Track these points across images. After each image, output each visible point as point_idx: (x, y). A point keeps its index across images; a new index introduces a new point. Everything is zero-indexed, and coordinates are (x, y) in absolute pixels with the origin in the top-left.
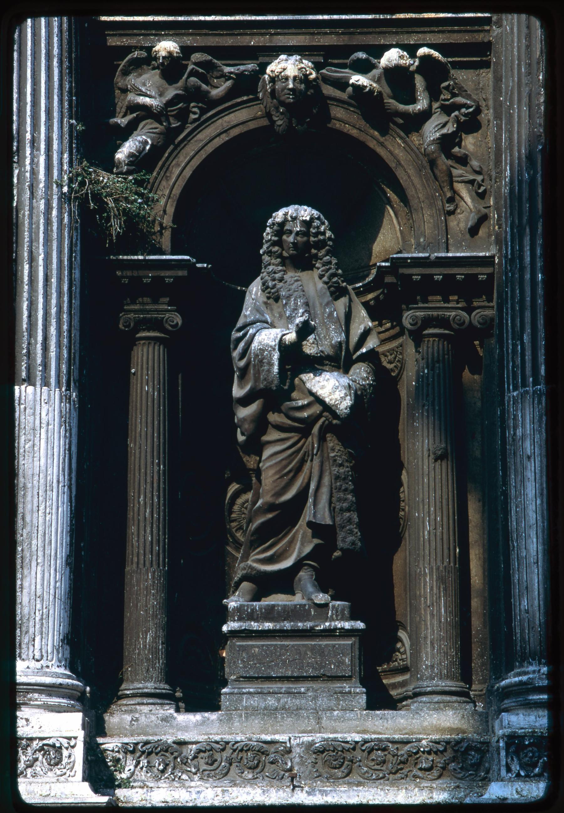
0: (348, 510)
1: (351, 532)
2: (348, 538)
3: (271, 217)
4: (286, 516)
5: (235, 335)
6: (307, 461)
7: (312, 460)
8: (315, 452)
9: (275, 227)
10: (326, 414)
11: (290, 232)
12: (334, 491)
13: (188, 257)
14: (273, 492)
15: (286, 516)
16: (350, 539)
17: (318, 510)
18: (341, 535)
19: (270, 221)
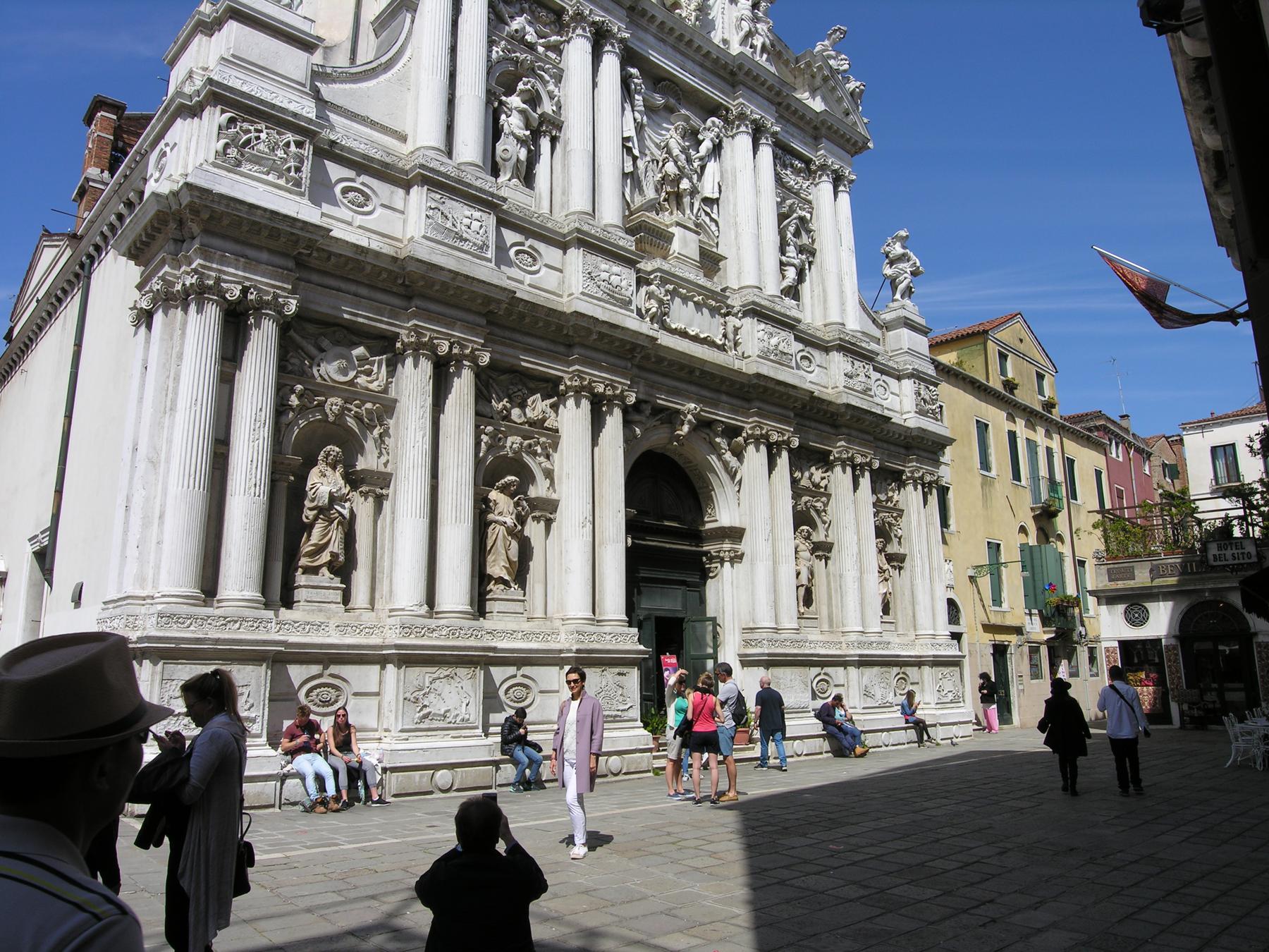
2: (342, 558)
4: (320, 549)
15: (320, 549)
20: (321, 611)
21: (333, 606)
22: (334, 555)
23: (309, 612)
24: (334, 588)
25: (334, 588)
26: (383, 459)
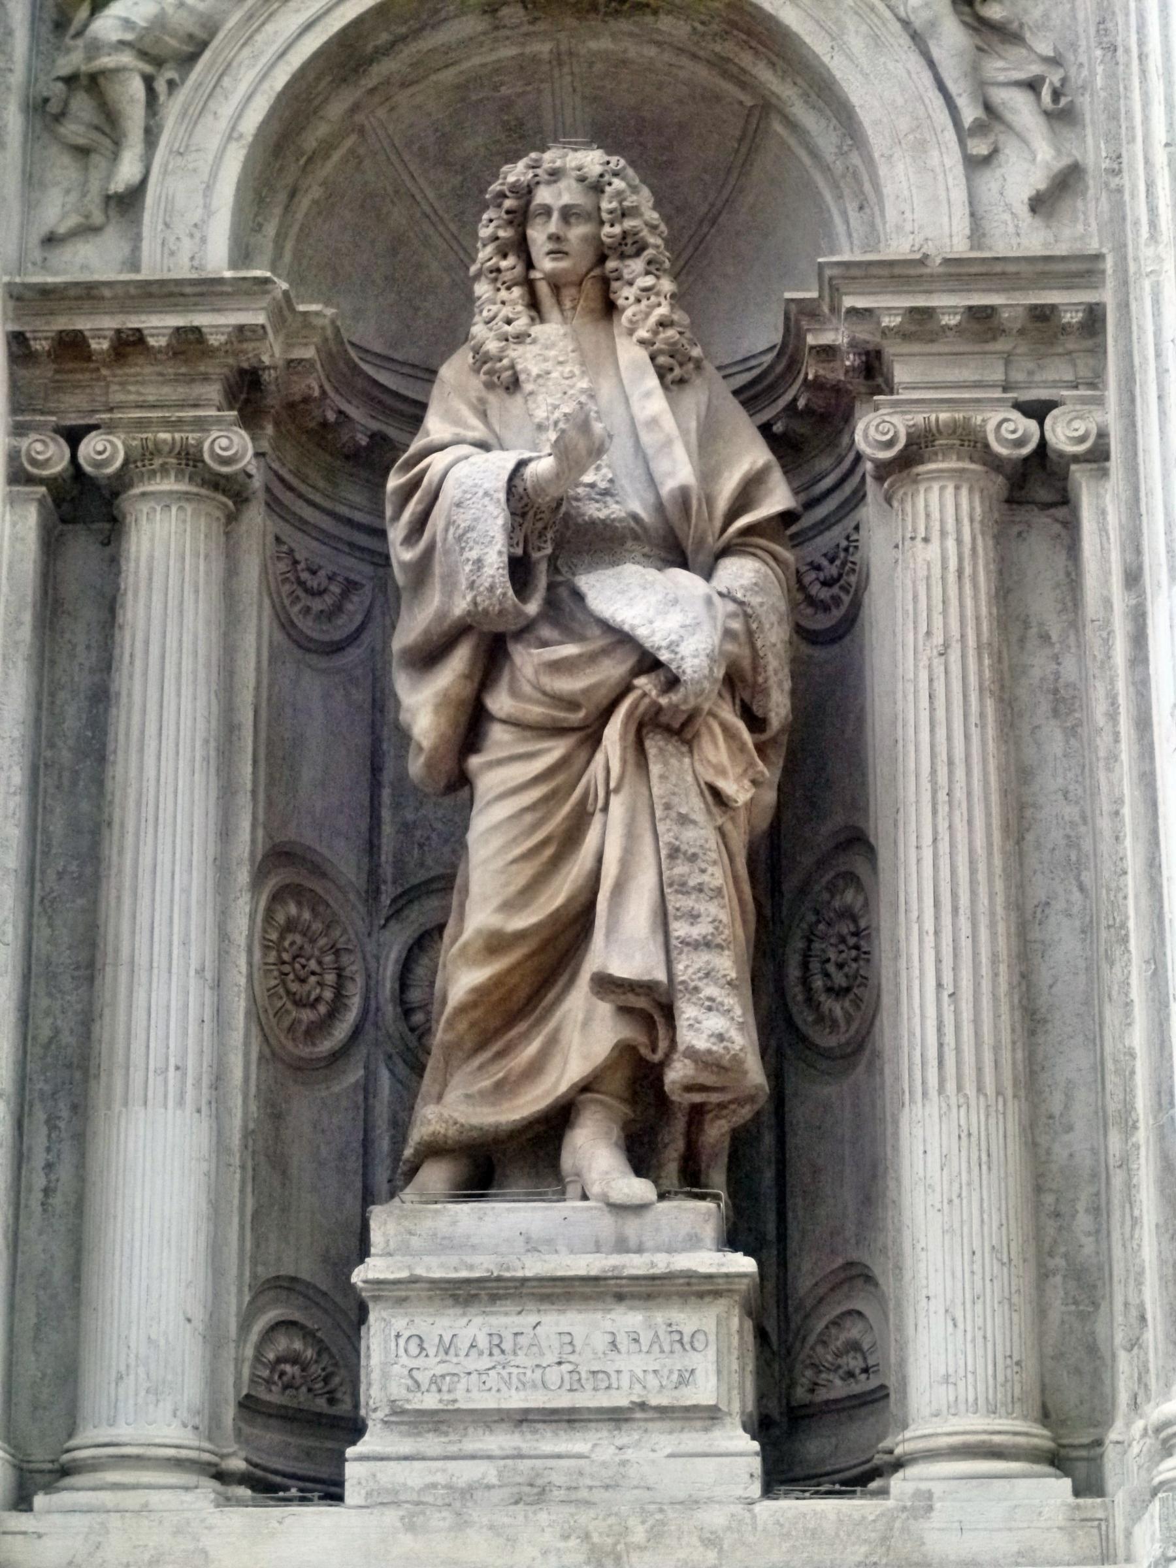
0: (706, 944)
1: (711, 1006)
3: (497, 177)
5: (394, 481)
6: (593, 814)
7: (605, 809)
8: (612, 785)
9: (508, 203)
10: (641, 681)
11: (547, 211)
12: (667, 890)
13: (268, 274)
14: (496, 902)
16: (715, 1023)
17: (624, 948)
18: (687, 1012)
19: (495, 187)
20: (536, 1494)
21: (652, 1454)
22: (650, 1008)
23: (413, 1509)
26: (1025, 169)
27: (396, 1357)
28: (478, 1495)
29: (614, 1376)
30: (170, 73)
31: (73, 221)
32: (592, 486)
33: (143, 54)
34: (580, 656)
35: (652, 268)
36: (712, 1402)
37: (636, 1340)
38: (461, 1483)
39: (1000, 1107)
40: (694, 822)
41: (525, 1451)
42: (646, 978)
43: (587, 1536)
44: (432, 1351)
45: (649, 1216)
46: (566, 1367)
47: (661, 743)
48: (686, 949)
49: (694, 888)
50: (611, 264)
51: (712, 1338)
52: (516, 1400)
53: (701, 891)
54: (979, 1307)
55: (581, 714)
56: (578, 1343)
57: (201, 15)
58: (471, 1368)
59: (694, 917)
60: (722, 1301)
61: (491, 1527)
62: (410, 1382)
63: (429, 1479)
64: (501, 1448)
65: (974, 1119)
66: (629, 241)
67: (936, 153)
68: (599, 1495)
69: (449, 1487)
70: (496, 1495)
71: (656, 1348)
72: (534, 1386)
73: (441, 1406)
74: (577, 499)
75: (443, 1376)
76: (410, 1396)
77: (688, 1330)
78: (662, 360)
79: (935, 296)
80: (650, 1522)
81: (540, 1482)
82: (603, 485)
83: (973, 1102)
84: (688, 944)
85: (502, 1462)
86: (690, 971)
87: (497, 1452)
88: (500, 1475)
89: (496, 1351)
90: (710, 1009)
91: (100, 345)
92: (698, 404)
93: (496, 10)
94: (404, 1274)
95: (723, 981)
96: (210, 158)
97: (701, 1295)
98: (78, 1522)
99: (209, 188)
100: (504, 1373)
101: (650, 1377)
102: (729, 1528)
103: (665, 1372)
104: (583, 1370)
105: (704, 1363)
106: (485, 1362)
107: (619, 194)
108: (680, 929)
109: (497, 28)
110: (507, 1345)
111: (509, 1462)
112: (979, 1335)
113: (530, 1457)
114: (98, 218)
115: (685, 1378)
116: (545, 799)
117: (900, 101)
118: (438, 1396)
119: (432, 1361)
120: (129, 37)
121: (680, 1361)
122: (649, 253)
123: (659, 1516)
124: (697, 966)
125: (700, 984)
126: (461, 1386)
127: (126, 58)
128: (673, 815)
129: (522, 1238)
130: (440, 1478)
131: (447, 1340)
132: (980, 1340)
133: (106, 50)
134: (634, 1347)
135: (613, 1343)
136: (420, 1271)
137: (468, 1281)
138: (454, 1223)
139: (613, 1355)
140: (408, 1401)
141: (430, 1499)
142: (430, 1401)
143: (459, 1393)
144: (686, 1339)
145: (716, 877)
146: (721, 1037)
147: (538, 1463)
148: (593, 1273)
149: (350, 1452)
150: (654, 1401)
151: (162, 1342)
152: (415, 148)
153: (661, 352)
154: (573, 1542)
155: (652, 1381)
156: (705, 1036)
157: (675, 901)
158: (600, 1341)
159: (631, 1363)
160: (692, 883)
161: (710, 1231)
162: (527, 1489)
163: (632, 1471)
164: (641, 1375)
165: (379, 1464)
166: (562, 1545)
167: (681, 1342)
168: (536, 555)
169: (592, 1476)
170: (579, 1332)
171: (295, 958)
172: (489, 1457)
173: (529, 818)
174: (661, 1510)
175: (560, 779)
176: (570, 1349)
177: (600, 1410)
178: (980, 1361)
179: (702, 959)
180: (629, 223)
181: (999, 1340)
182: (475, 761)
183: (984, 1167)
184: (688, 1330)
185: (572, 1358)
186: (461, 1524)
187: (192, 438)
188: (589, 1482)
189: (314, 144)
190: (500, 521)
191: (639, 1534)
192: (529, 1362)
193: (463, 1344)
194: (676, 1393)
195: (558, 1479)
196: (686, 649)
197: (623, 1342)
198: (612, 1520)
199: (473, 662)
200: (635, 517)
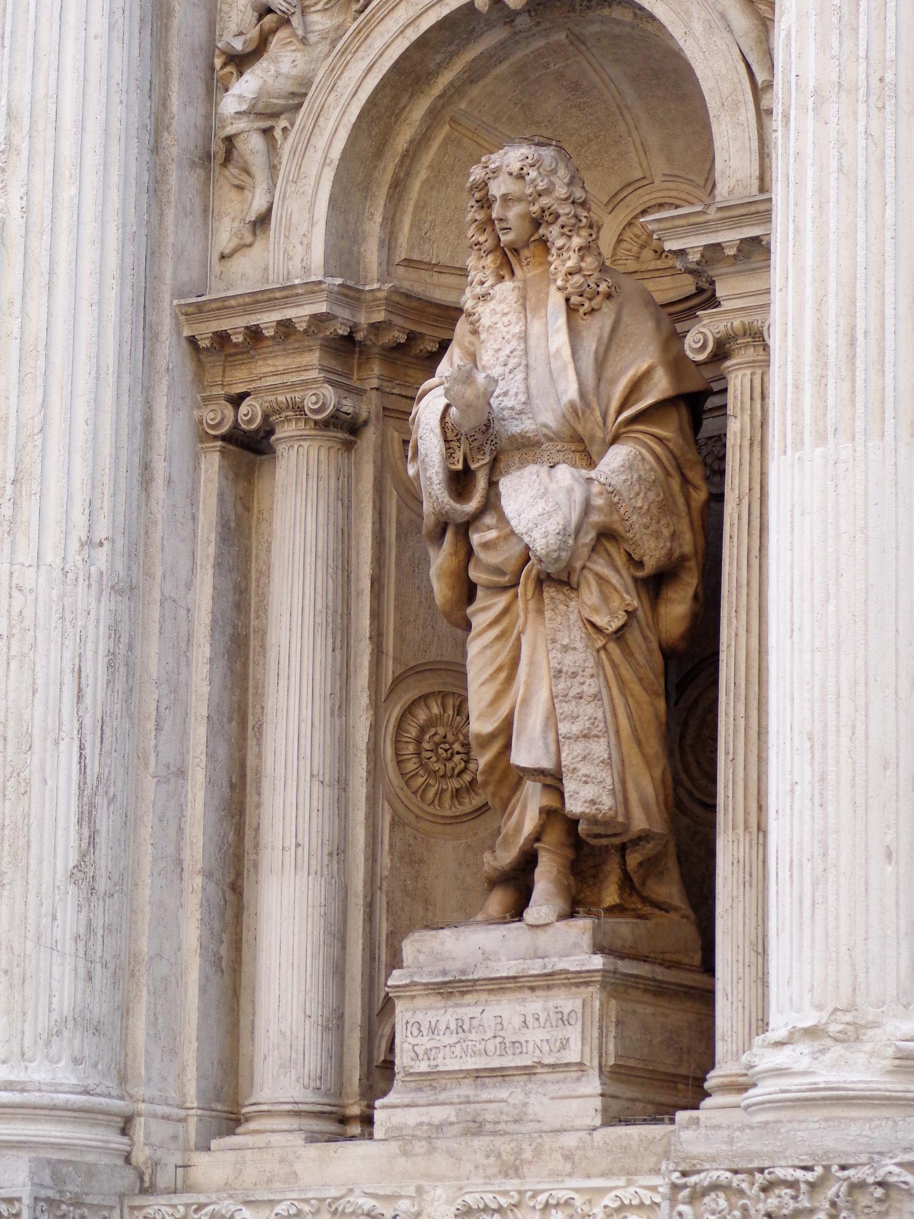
16: (588, 792)
18: (569, 786)
20: (475, 1128)
24: (548, 981)
25: (548, 981)
27: (423, 1035)
28: (445, 1129)
29: (524, 1044)
30: (283, 123)
31: (235, 242)
32: (512, 408)
33: (260, 115)
34: (498, 538)
35: (566, 230)
36: (578, 1060)
37: (538, 1019)
38: (436, 1121)
39: (761, 841)
40: (575, 649)
41: (472, 1099)
42: (537, 766)
43: (499, 1156)
44: (425, 1033)
45: (550, 930)
46: (499, 1040)
47: (553, 594)
48: (568, 741)
49: (575, 697)
50: (541, 231)
51: (580, 1015)
52: (471, 1063)
53: (581, 698)
54: (741, 986)
55: (507, 578)
56: (505, 1023)
57: (295, 78)
58: (446, 1043)
59: (574, 718)
60: (591, 989)
61: (448, 1152)
62: (413, 1054)
63: (419, 1120)
64: (459, 1096)
65: (741, 853)
66: (547, 213)
67: (743, 111)
68: (511, 1127)
69: (429, 1124)
70: (457, 1129)
71: (548, 1024)
72: (480, 1054)
73: (429, 1070)
74: (504, 420)
75: (431, 1049)
76: (412, 1063)
77: (566, 1011)
78: (575, 299)
79: (720, 233)
80: (534, 1145)
81: (479, 1119)
82: (518, 407)
83: (741, 839)
84: (569, 738)
85: (458, 1107)
86: (570, 757)
87: (456, 1100)
88: (457, 1115)
89: (460, 1030)
90: (586, 782)
91: (238, 339)
92: (601, 329)
93: (513, 21)
94: (407, 981)
95: (598, 761)
96: (312, 183)
97: (578, 985)
98: (231, 1156)
99: (313, 205)
100: (464, 1045)
101: (545, 1043)
102: (578, 1147)
103: (552, 1041)
104: (507, 1041)
105: (574, 1033)
106: (453, 1039)
107: (533, 181)
108: (563, 728)
109: (515, 33)
110: (466, 1027)
111: (462, 1106)
112: (740, 1005)
113: (474, 1102)
114: (248, 239)
115: (564, 1044)
116: (498, 638)
117: (724, 71)
118: (427, 1063)
119: (426, 1039)
120: (244, 107)
121: (561, 1033)
122: (562, 220)
123: (539, 1140)
124: (575, 754)
125: (579, 766)
126: (441, 1055)
127: (242, 125)
128: (558, 646)
129: (480, 951)
130: (425, 1119)
131: (433, 1024)
132: (741, 1009)
133: (229, 121)
134: (536, 1024)
135: (525, 1022)
136: (417, 979)
137: (444, 983)
138: (442, 943)
139: (524, 1030)
140: (412, 1067)
141: (419, 1133)
142: (423, 1067)
143: (440, 1061)
144: (565, 1017)
145: (591, 687)
146: (593, 802)
147: (478, 1106)
148: (511, 974)
149: (378, 1103)
150: (546, 1062)
151: (288, 1033)
152: (505, 119)
153: (573, 294)
154: (492, 1160)
155: (546, 1048)
156: (580, 803)
157: (563, 708)
158: (517, 1021)
159: (536, 1035)
160: (574, 691)
161: (586, 941)
162: (471, 1124)
163: (530, 1110)
164: (539, 1043)
165: (392, 1110)
166: (485, 1162)
167: (562, 1019)
168: (473, 466)
169: (507, 1114)
170: (506, 1015)
171: (437, 745)
172: (452, 1103)
173: (489, 653)
174: (541, 1136)
175: (505, 623)
176: (500, 1027)
177: (517, 1068)
178: (740, 1024)
179: (579, 748)
180: (544, 201)
181: (754, 1009)
182: (470, 610)
183: (747, 885)
184: (566, 1011)
185: (502, 1033)
186: (432, 1150)
187: (297, 396)
188: (505, 1118)
189: (405, 146)
190: (438, 450)
191: (528, 1155)
192: (478, 1038)
193: (442, 1027)
194: (558, 1055)
195: (489, 1117)
196: (536, 534)
197: (530, 1019)
198: (513, 1144)
199: (456, 543)
200: (546, 426)
